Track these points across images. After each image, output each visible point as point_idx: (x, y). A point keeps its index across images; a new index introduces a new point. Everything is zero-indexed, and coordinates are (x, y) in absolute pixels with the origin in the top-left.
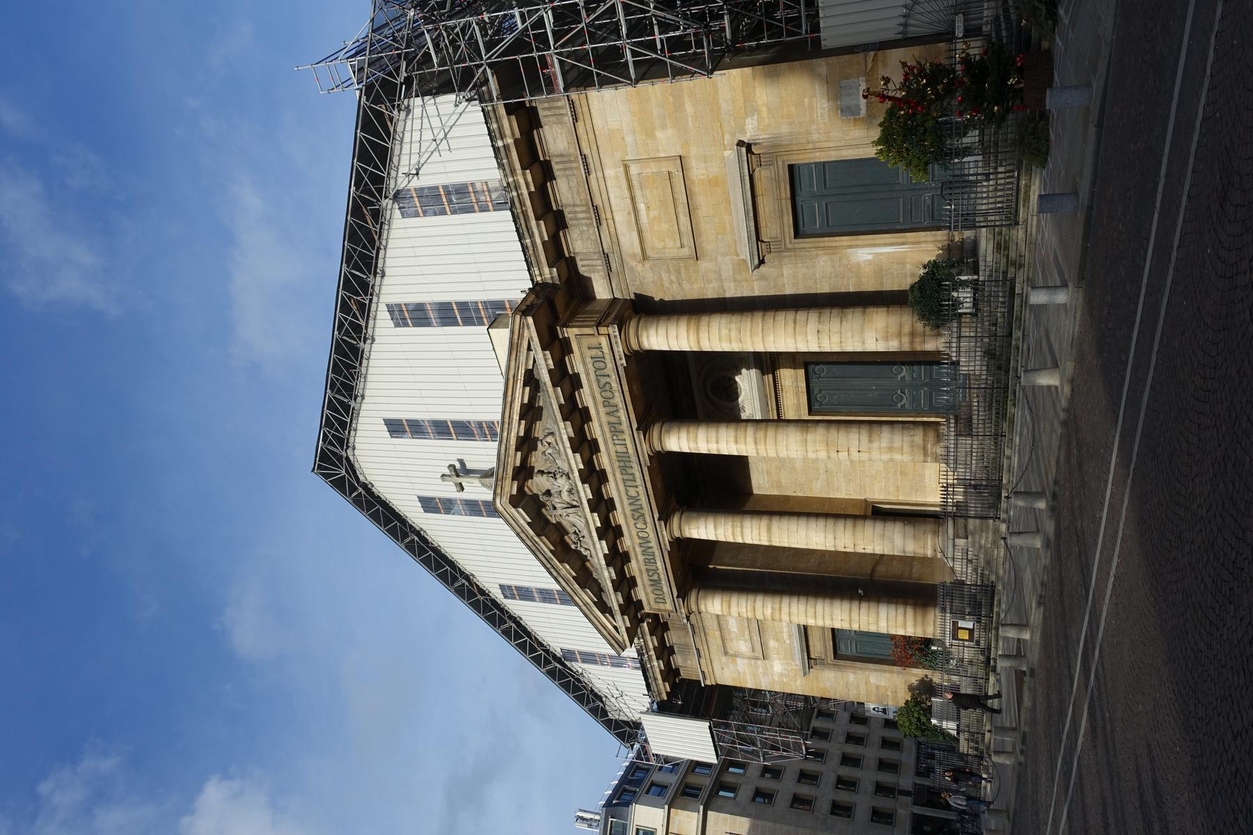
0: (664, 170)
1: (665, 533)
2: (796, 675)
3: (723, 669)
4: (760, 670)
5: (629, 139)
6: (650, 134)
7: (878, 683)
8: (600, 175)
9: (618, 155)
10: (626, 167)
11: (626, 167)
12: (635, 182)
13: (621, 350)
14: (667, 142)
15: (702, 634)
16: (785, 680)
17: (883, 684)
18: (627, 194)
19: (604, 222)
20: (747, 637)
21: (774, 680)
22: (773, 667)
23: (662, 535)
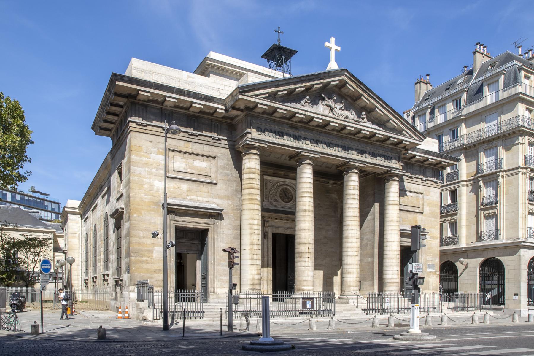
0: (420, 206)
1: (313, 155)
2: (153, 195)
3: (151, 142)
4: (154, 171)
5: (428, 197)
6: (428, 205)
7: (154, 252)
8: (421, 183)
9: (424, 192)
10: (422, 194)
11: (422, 194)
12: (418, 195)
13: (397, 172)
14: (426, 210)
15: (187, 139)
16: (145, 186)
17: (154, 255)
18: (415, 191)
19: (409, 179)
20: (189, 171)
21: (144, 178)
22: (159, 181)
23: (312, 154)
